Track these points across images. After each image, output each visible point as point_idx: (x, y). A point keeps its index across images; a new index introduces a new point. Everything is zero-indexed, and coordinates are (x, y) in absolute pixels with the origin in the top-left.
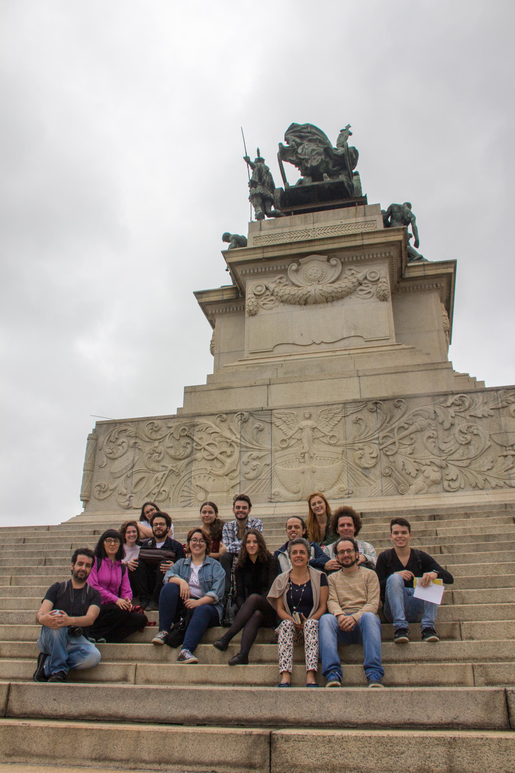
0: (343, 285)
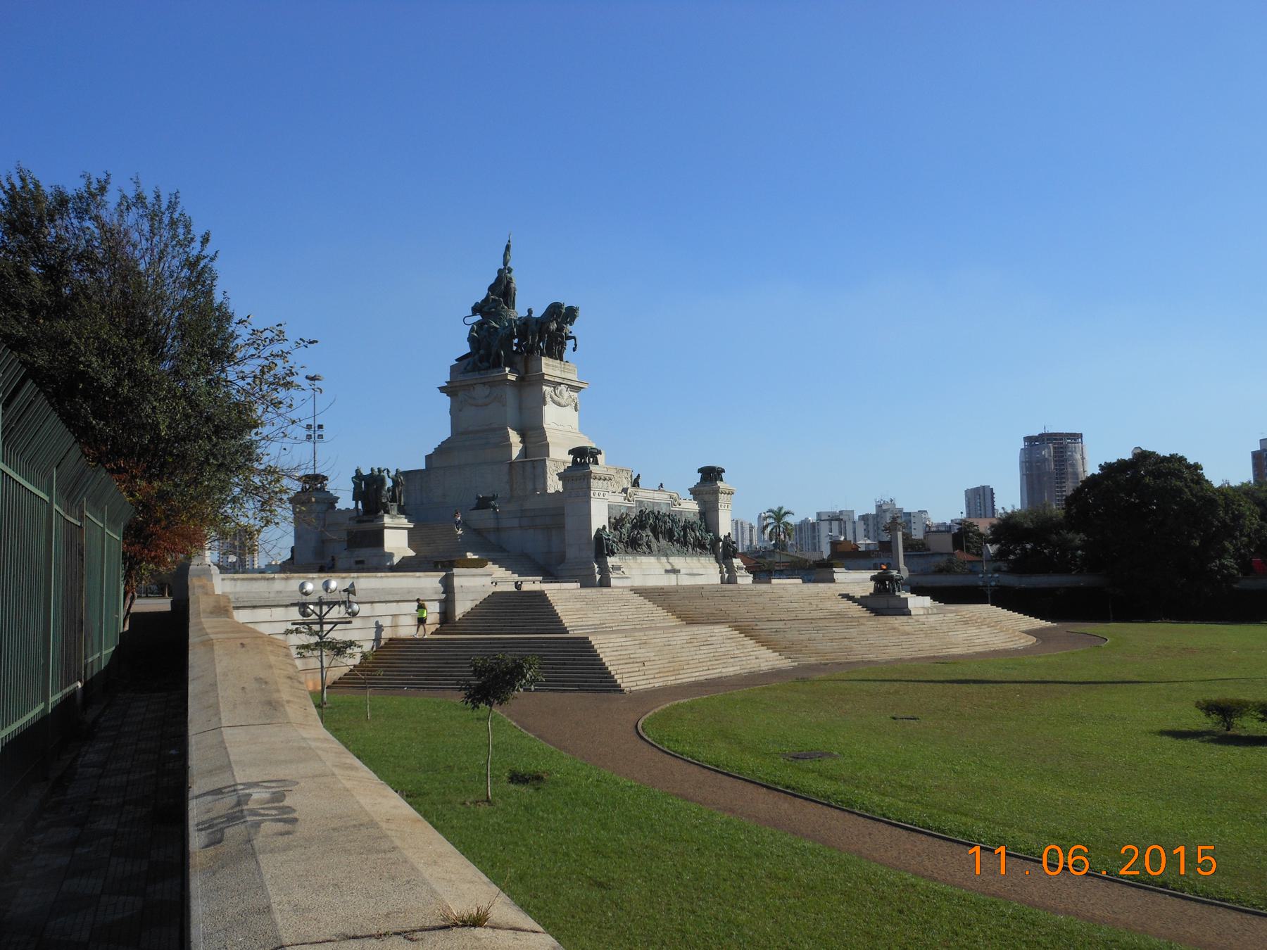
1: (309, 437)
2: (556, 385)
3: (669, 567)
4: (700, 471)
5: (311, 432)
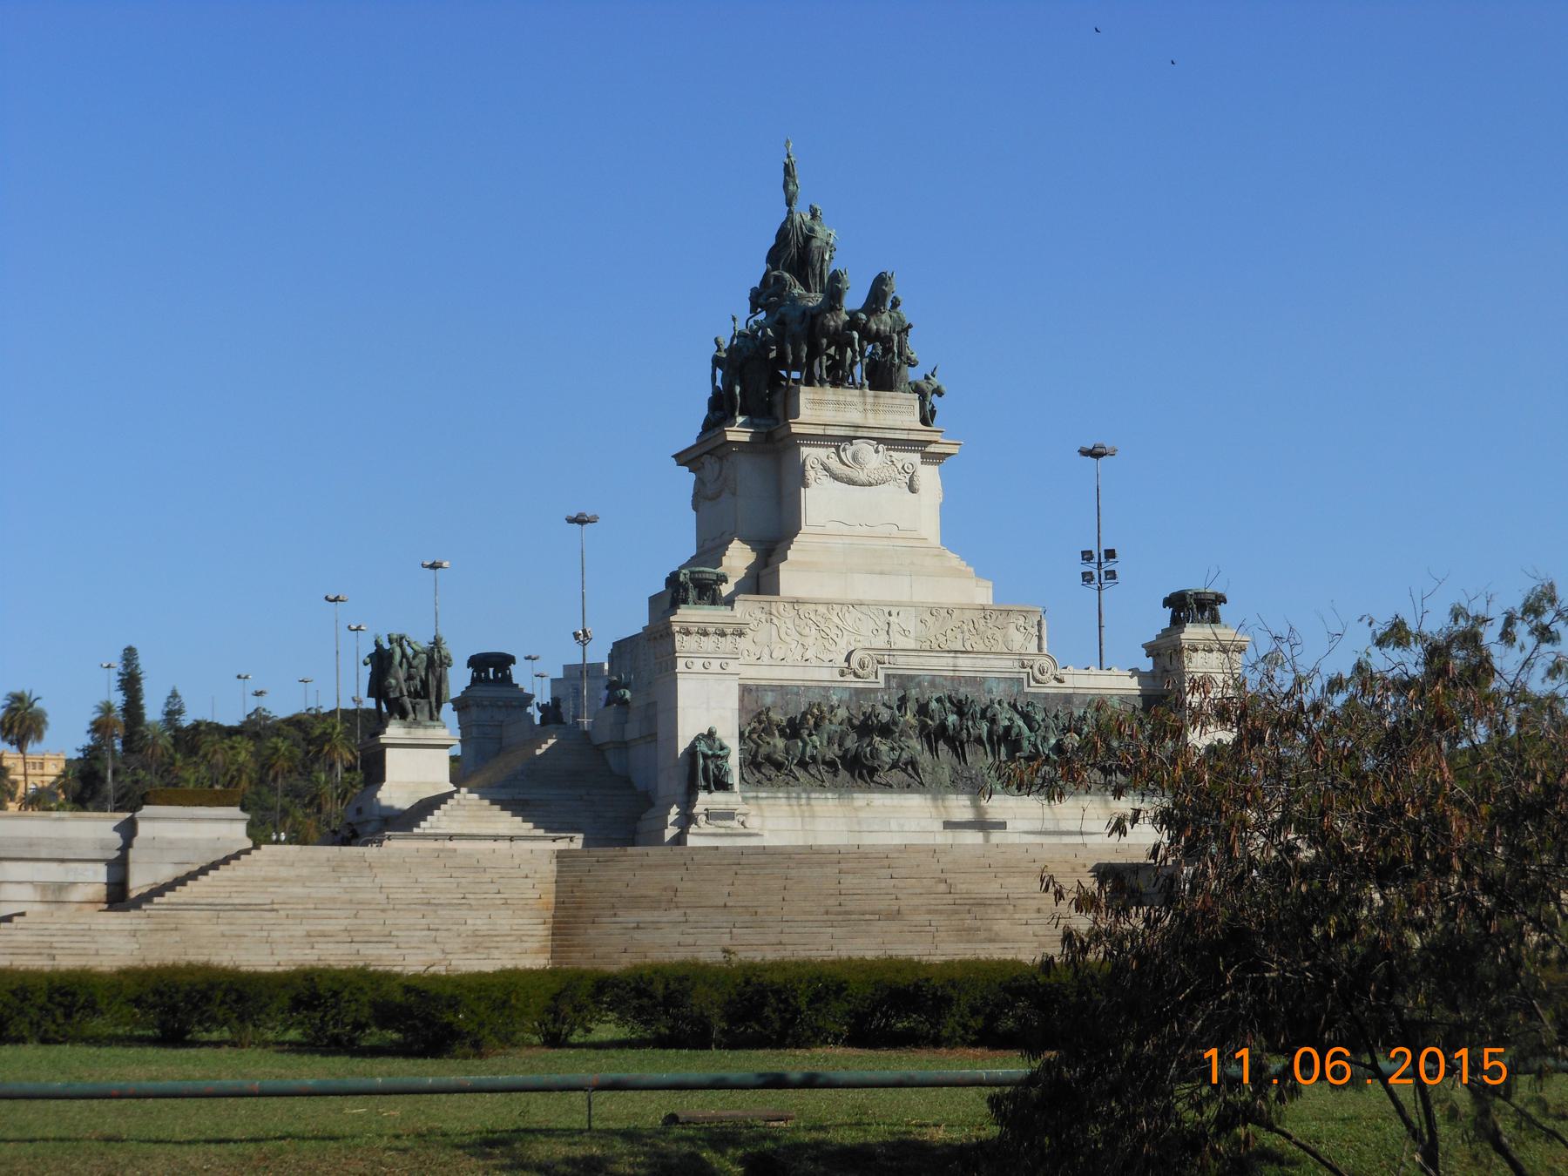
1: (1087, 577)
2: (838, 442)
3: (967, 815)
4: (1168, 602)
5: (1092, 567)
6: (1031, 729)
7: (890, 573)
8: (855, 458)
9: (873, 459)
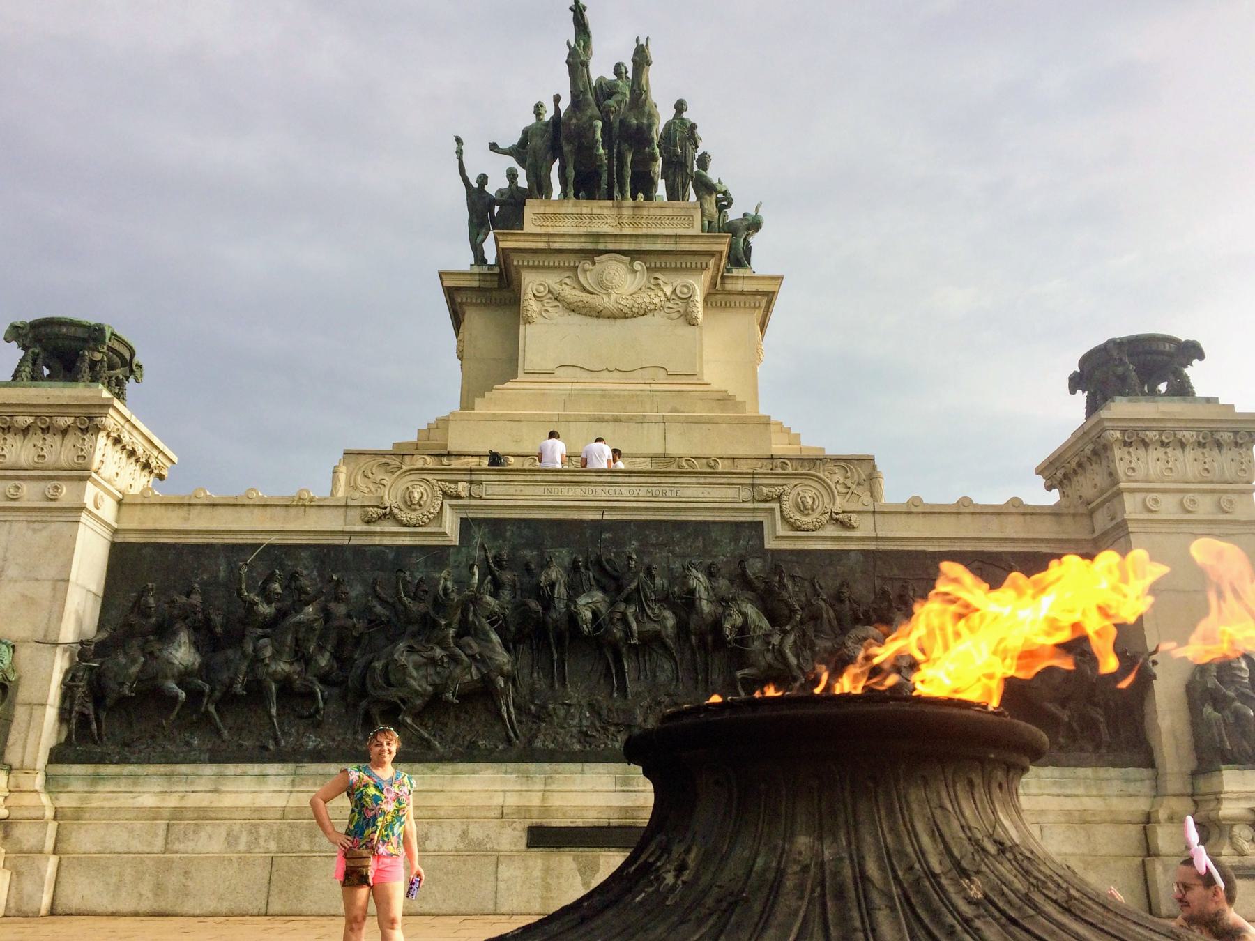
0: (647, 300)
6: (773, 620)
7: (629, 420)
8: (600, 282)
9: (623, 282)
